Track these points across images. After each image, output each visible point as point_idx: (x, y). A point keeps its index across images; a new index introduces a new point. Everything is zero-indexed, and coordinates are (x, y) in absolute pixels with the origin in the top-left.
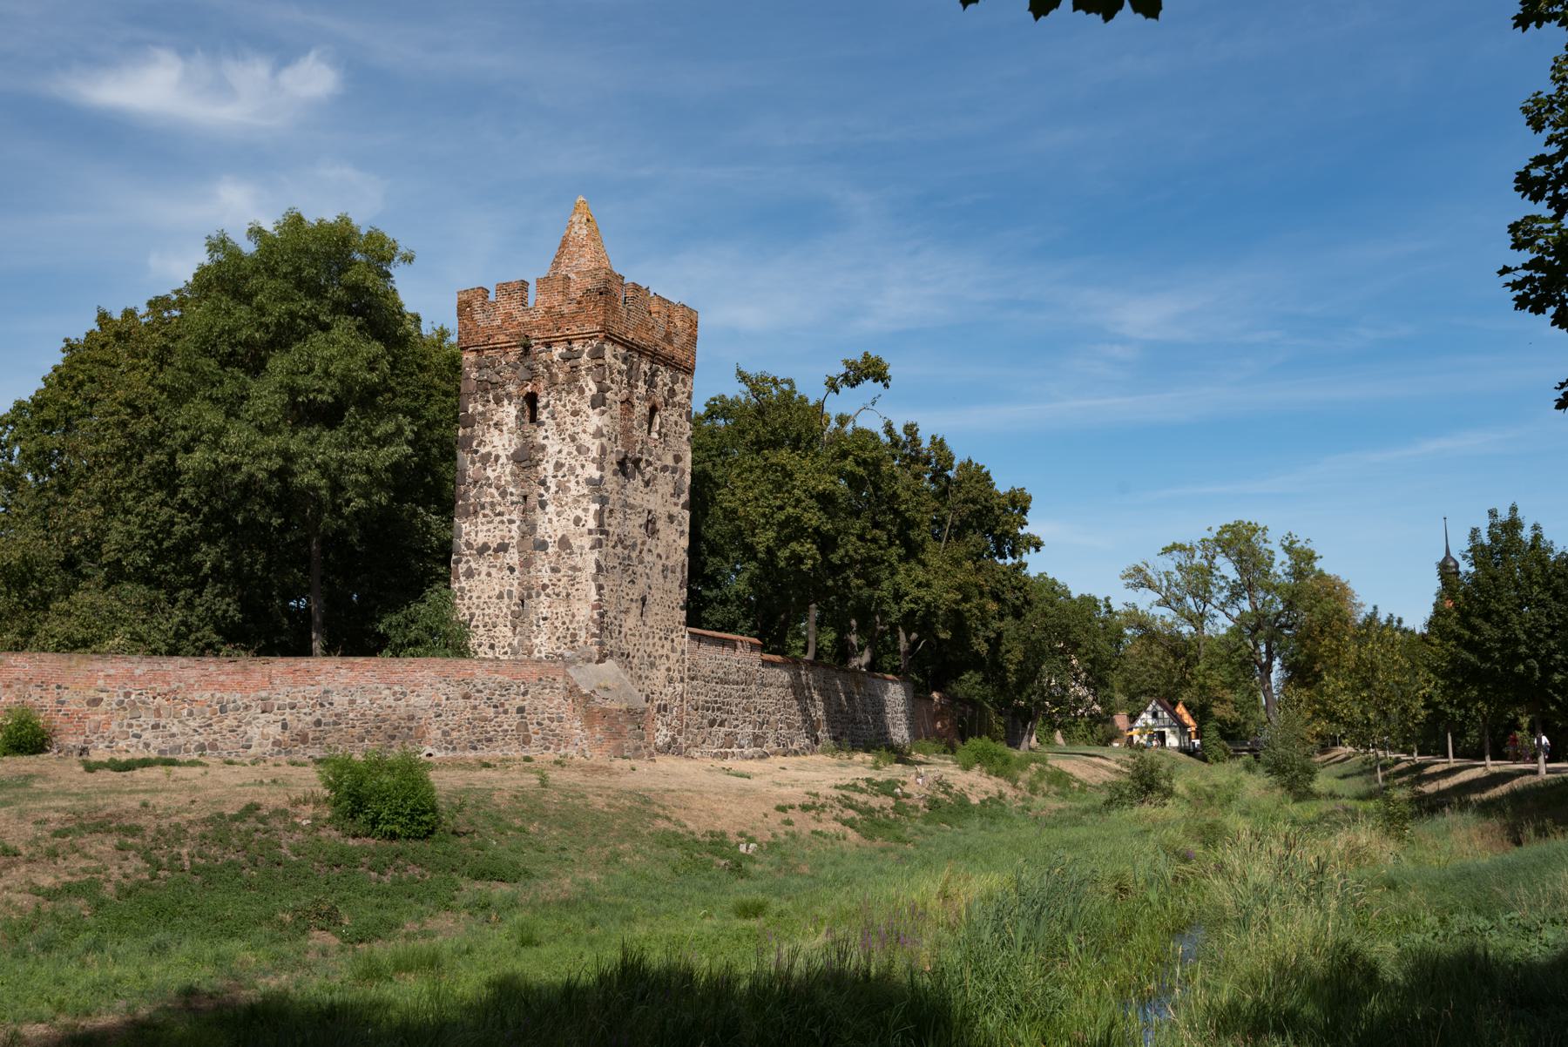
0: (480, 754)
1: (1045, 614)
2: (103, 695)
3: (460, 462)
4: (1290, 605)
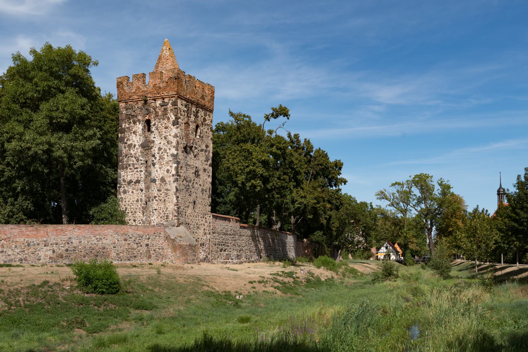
0: (131, 262)
1: (347, 209)
3: (119, 147)
4: (440, 206)
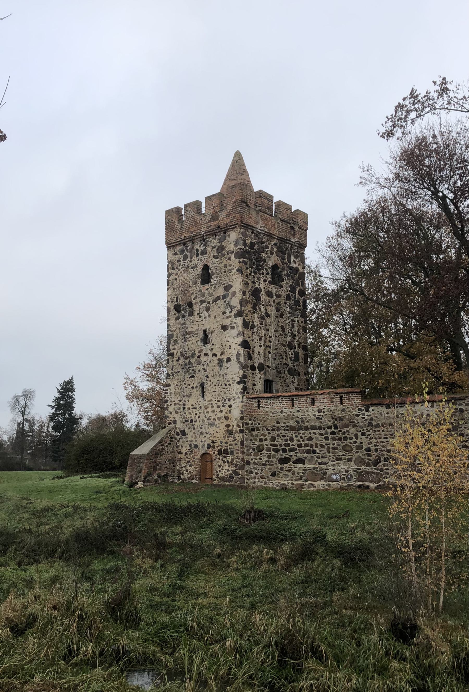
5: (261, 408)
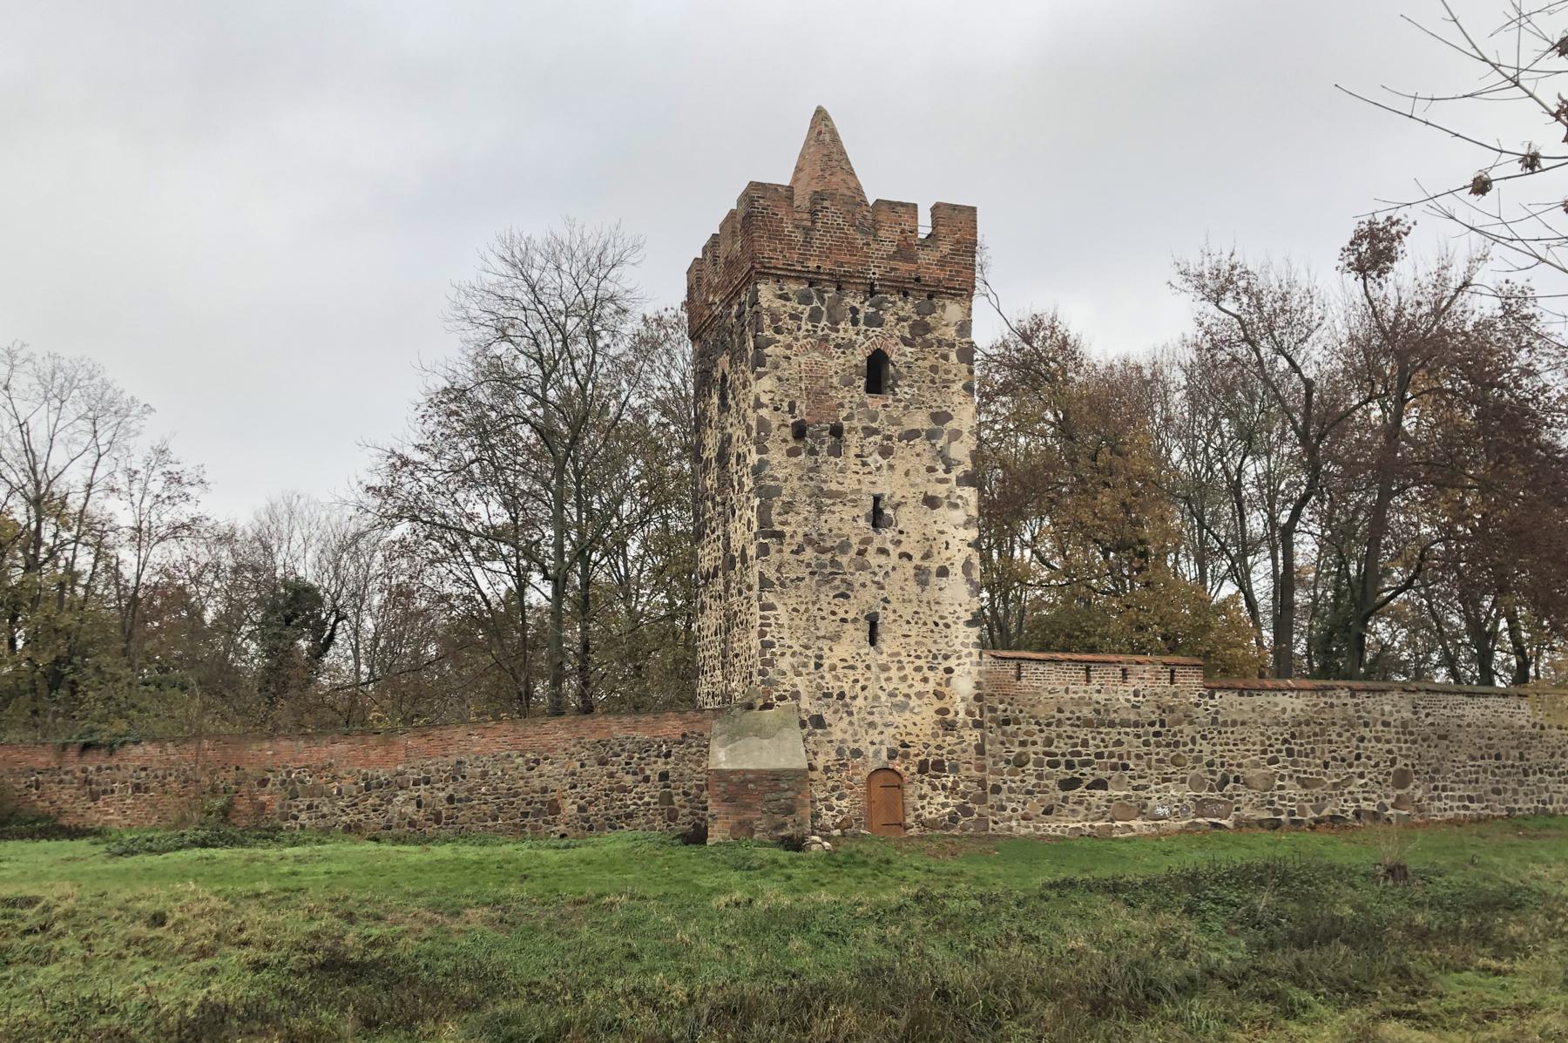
2: (270, 775)
5: (1024, 681)
